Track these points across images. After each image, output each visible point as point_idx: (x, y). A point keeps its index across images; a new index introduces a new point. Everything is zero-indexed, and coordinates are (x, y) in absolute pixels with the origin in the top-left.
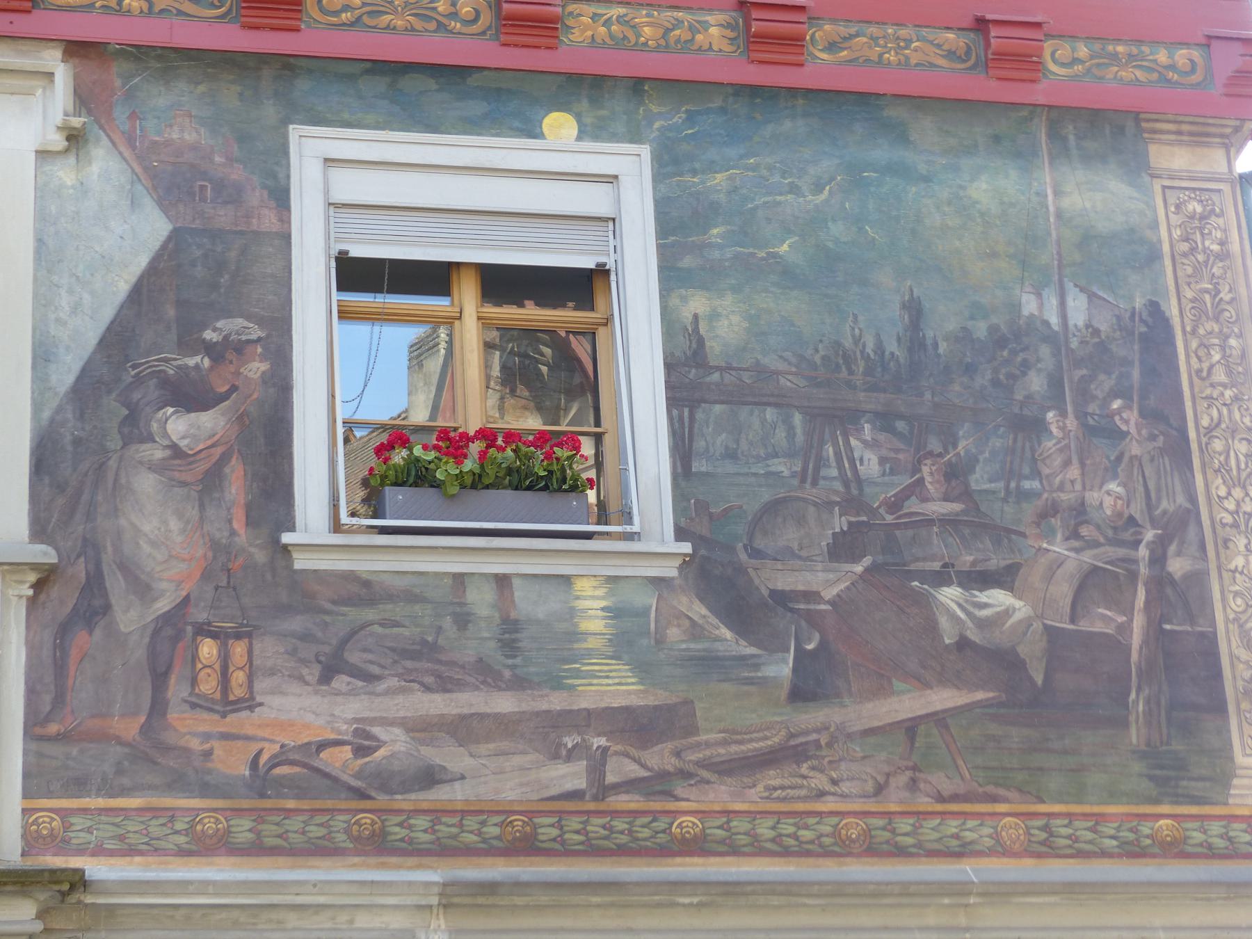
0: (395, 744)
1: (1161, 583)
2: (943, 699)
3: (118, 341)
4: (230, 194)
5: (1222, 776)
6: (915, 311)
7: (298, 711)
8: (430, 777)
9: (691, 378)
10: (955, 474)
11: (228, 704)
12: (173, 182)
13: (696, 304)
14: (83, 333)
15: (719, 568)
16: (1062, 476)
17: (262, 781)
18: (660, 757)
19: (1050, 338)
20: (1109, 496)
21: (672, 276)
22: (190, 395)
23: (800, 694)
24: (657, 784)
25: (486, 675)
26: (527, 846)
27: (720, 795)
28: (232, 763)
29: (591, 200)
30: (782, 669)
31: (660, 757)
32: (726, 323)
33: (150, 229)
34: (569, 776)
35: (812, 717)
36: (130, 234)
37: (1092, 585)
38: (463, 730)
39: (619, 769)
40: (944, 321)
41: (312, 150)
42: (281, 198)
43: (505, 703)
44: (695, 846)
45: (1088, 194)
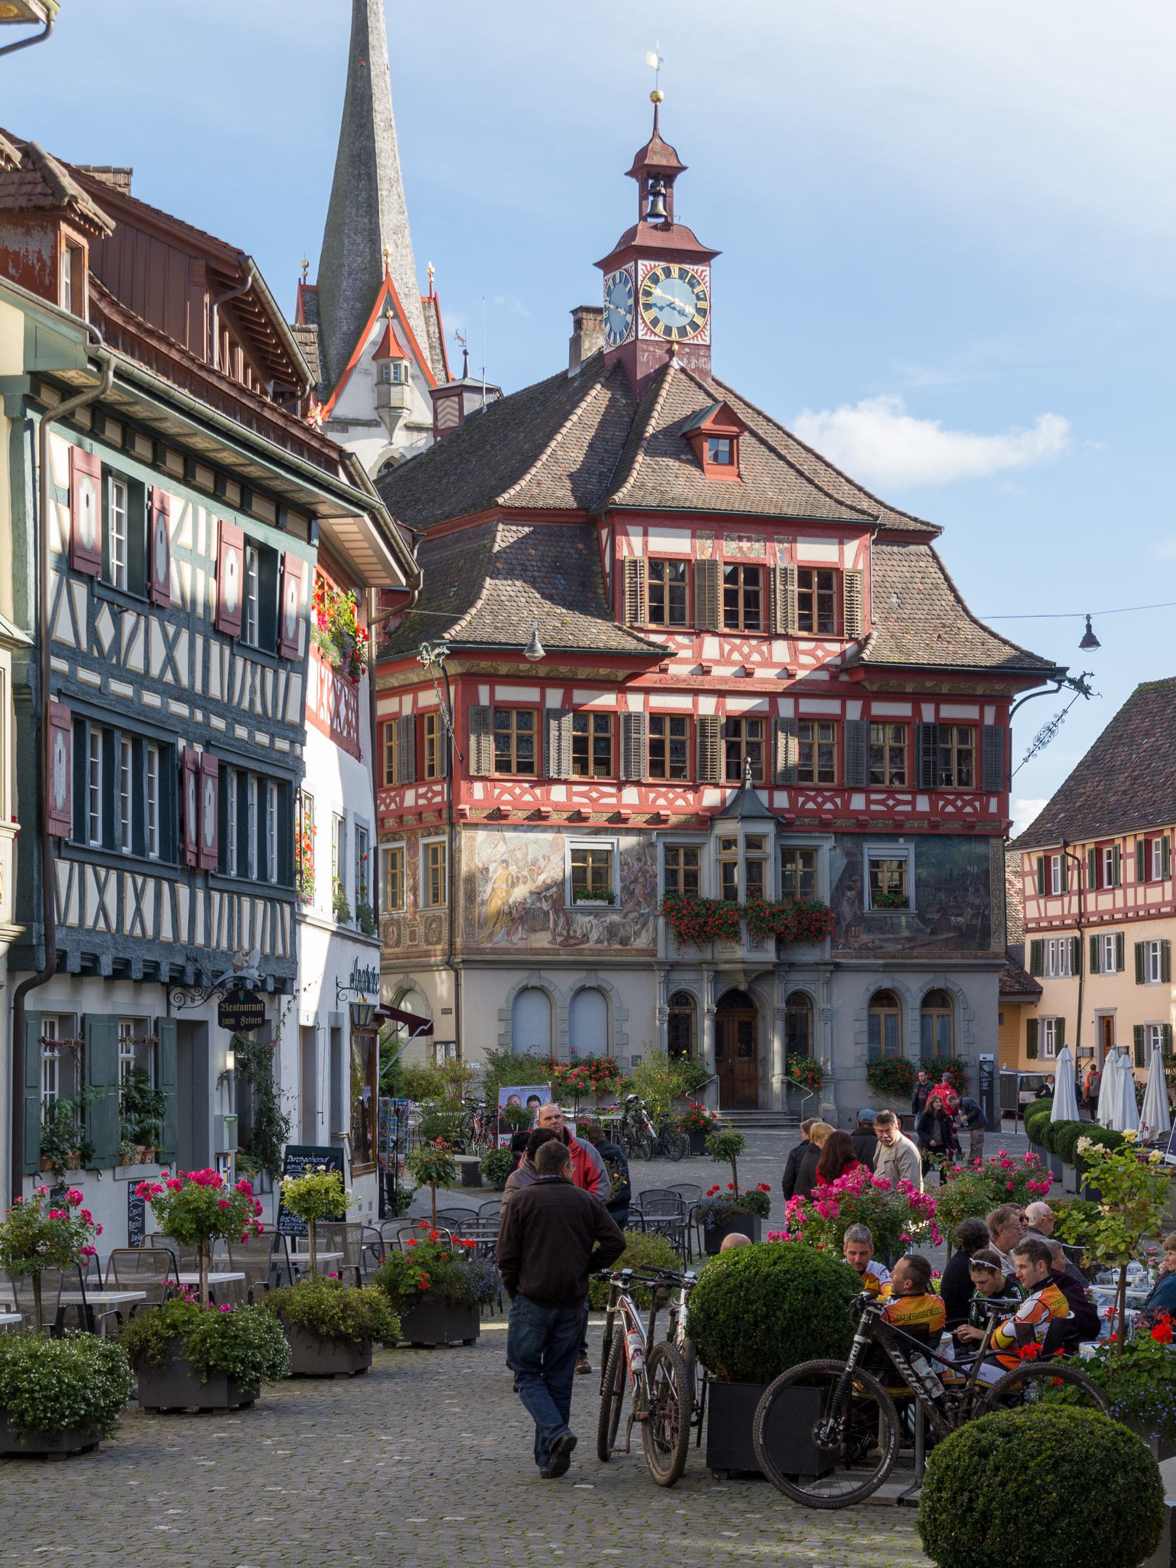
0: (877, 942)
1: (984, 915)
2: (951, 935)
3: (841, 880)
4: (855, 855)
5: (989, 947)
6: (951, 870)
7: (865, 938)
8: (882, 947)
9: (919, 882)
10: (955, 898)
11: (856, 937)
12: (848, 854)
13: (920, 871)
14: (836, 879)
15: (921, 915)
16: (971, 898)
17: (860, 948)
18: (912, 944)
19: (972, 875)
20: (977, 901)
21: (917, 866)
22: (850, 889)
23: (932, 933)
24: (911, 948)
25: (889, 932)
26: (894, 957)
27: (920, 950)
28: (857, 946)
29: (904, 853)
30: (929, 931)
31: (912, 944)
32: (924, 873)
33: (845, 861)
34: (900, 947)
35: (934, 937)
36: (842, 862)
37: (974, 916)
38: (886, 940)
39: (907, 946)
40: (956, 872)
41: (866, 845)
42: (862, 855)
43: (891, 936)
44: (916, 957)
45: (979, 849)
